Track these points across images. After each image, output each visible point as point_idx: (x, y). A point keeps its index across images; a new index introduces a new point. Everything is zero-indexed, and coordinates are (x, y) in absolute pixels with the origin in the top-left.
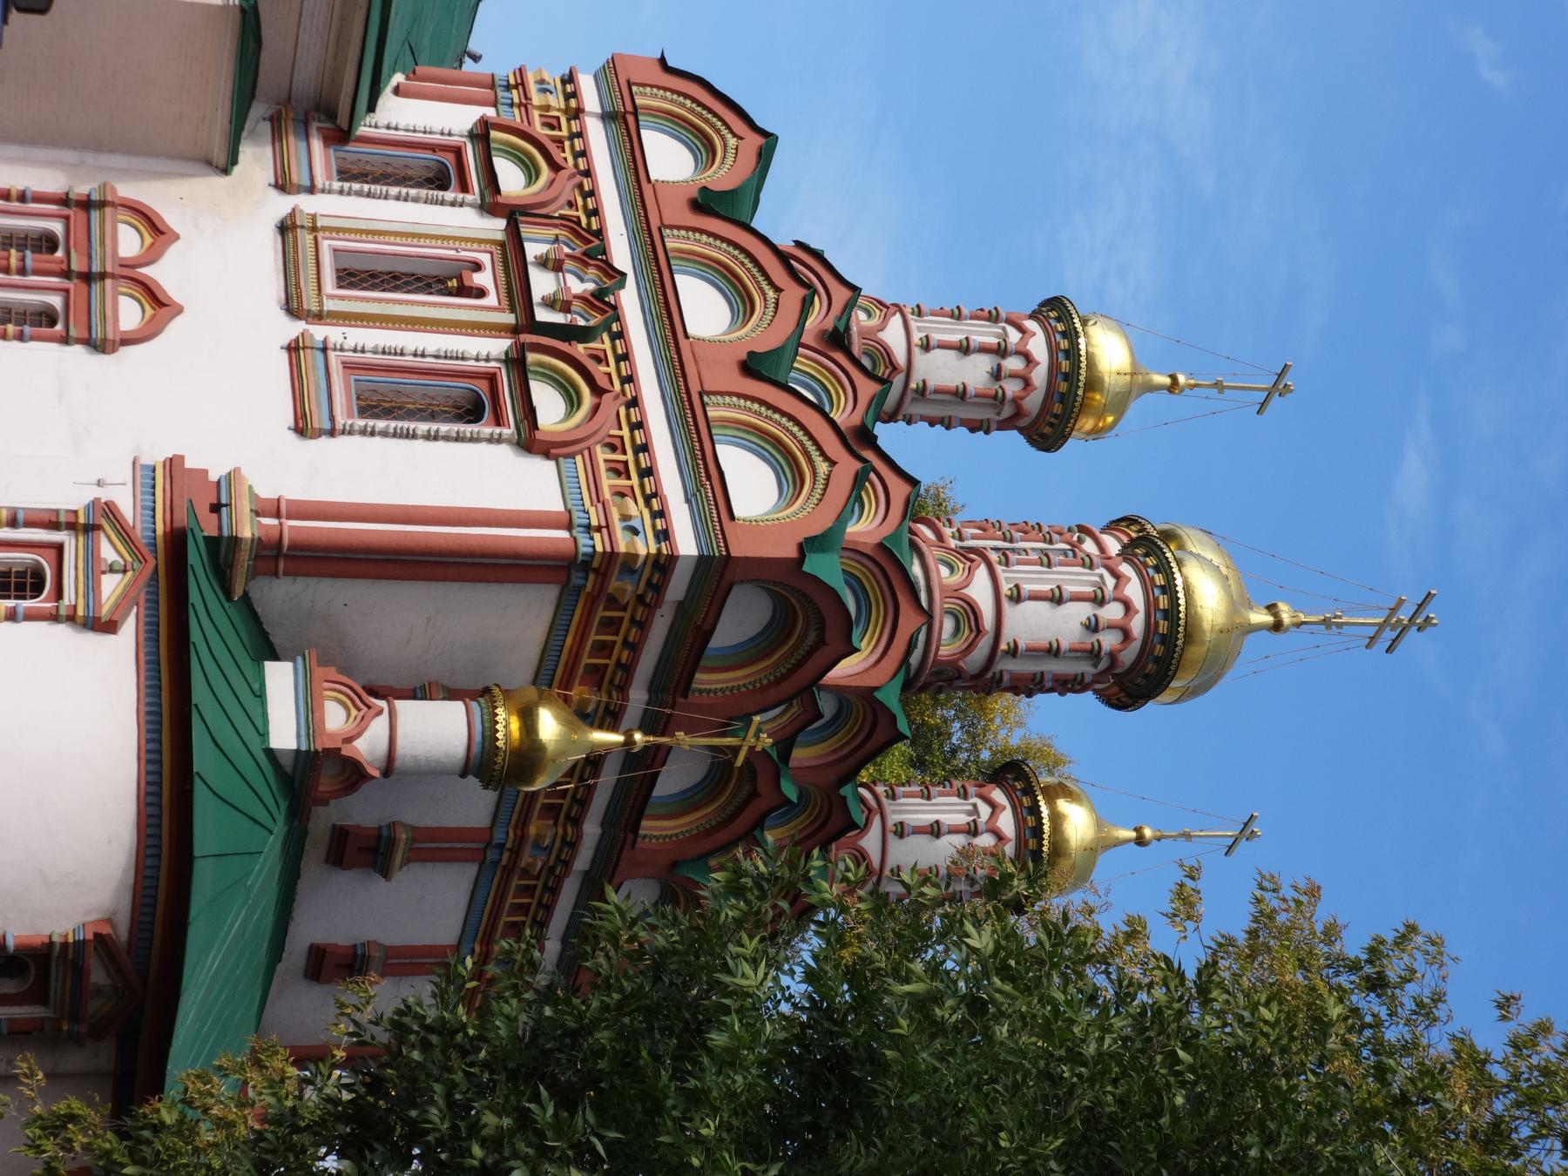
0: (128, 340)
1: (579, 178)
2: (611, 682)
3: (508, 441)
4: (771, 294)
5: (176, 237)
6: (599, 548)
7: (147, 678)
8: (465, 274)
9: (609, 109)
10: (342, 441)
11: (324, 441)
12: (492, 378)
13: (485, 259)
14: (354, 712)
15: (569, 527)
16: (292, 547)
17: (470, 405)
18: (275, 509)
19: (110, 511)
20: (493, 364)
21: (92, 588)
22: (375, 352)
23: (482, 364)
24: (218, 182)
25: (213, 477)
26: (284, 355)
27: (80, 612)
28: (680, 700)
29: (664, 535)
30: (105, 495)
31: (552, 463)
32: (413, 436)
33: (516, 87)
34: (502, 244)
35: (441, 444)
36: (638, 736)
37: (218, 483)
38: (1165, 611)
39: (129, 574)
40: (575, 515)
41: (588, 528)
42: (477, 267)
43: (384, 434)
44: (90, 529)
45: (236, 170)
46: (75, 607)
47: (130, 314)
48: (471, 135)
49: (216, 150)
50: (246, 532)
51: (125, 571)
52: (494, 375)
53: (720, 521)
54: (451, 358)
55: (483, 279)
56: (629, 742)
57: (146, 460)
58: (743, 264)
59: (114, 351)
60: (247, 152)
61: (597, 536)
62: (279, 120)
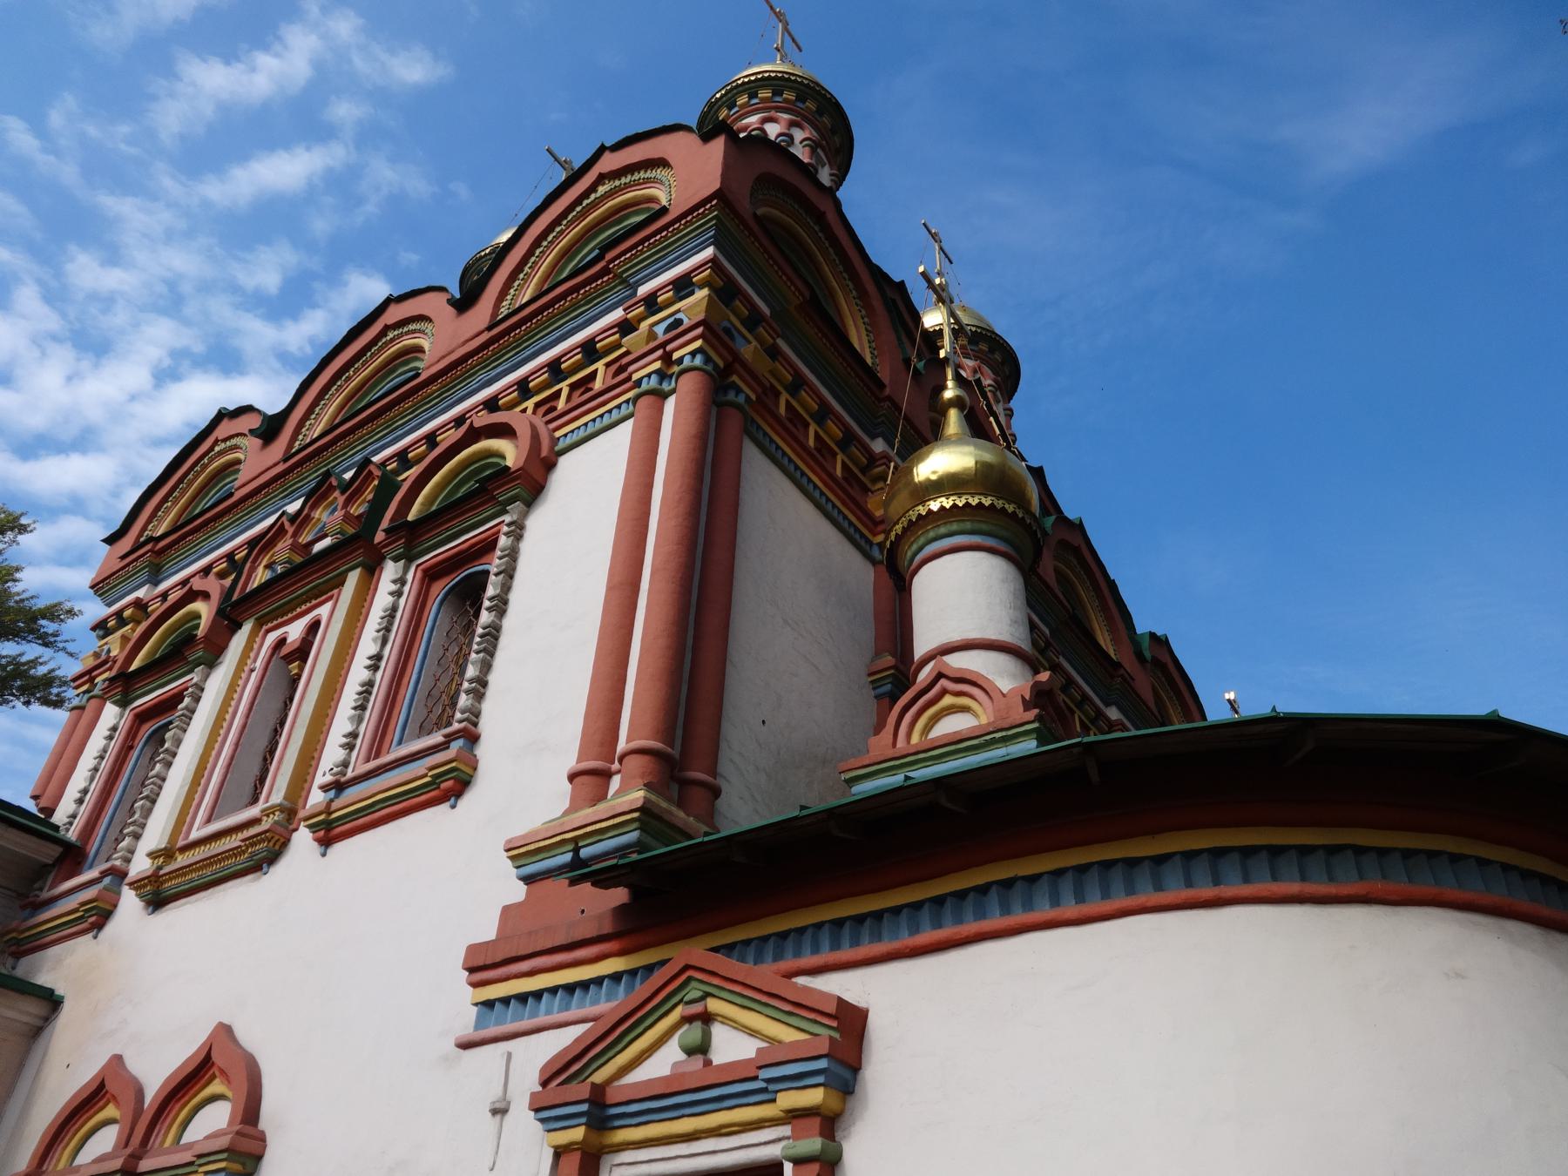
0: (250, 1112)
1: (211, 577)
2: (864, 470)
3: (525, 515)
4: (391, 335)
5: (117, 1060)
6: (699, 343)
7: (981, 914)
8: (285, 651)
9: (144, 575)
10: (486, 726)
11: (483, 751)
12: (431, 575)
13: (272, 637)
14: (948, 700)
15: (664, 396)
16: (667, 733)
17: (467, 594)
18: (590, 780)
19: (558, 1072)
20: (410, 576)
21: (748, 1084)
22: (360, 720)
23: (406, 589)
24: (67, 1007)
25: (517, 892)
26: (339, 848)
27: (813, 1097)
28: (887, 391)
29: (683, 286)
30: (527, 1081)
31: (563, 461)
32: (493, 633)
33: (92, 680)
34: (260, 623)
35: (513, 597)
36: (949, 394)
37: (528, 880)
38: (775, 94)
39: (714, 1005)
40: (644, 386)
41: (662, 375)
42: (282, 642)
43: (486, 667)
44: (601, 1113)
45: (59, 992)
46: (794, 1116)
47: (212, 1121)
48: (123, 704)
49: (10, 1014)
50: (637, 796)
51: (707, 1018)
52: (425, 571)
53: (665, 227)
54: (390, 623)
55: (295, 631)
56: (957, 402)
57: (465, 1019)
58: (349, 378)
59: (262, 1139)
60: (44, 979)
61: (676, 356)
62: (18, 942)
